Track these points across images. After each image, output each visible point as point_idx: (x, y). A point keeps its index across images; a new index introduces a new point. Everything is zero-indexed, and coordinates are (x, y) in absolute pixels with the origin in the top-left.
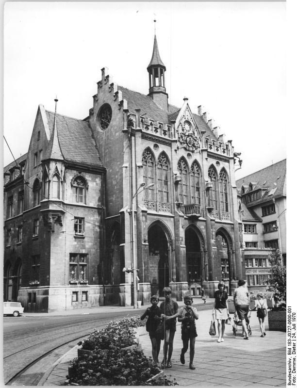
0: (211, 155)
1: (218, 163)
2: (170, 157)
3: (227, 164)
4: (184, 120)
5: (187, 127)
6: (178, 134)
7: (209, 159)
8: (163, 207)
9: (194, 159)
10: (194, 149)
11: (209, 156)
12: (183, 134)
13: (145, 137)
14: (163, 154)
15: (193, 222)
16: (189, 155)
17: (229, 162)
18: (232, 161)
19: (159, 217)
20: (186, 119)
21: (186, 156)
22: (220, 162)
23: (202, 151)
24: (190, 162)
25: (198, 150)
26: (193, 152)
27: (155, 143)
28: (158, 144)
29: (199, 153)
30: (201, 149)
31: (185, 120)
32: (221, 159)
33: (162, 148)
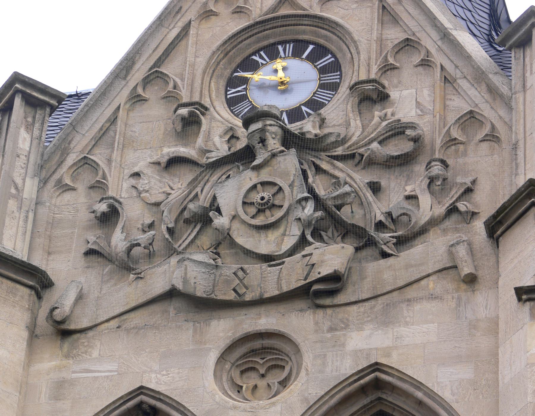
5: (285, 81)
6: (99, 186)
10: (332, 256)
12: (175, 162)
26: (320, 292)
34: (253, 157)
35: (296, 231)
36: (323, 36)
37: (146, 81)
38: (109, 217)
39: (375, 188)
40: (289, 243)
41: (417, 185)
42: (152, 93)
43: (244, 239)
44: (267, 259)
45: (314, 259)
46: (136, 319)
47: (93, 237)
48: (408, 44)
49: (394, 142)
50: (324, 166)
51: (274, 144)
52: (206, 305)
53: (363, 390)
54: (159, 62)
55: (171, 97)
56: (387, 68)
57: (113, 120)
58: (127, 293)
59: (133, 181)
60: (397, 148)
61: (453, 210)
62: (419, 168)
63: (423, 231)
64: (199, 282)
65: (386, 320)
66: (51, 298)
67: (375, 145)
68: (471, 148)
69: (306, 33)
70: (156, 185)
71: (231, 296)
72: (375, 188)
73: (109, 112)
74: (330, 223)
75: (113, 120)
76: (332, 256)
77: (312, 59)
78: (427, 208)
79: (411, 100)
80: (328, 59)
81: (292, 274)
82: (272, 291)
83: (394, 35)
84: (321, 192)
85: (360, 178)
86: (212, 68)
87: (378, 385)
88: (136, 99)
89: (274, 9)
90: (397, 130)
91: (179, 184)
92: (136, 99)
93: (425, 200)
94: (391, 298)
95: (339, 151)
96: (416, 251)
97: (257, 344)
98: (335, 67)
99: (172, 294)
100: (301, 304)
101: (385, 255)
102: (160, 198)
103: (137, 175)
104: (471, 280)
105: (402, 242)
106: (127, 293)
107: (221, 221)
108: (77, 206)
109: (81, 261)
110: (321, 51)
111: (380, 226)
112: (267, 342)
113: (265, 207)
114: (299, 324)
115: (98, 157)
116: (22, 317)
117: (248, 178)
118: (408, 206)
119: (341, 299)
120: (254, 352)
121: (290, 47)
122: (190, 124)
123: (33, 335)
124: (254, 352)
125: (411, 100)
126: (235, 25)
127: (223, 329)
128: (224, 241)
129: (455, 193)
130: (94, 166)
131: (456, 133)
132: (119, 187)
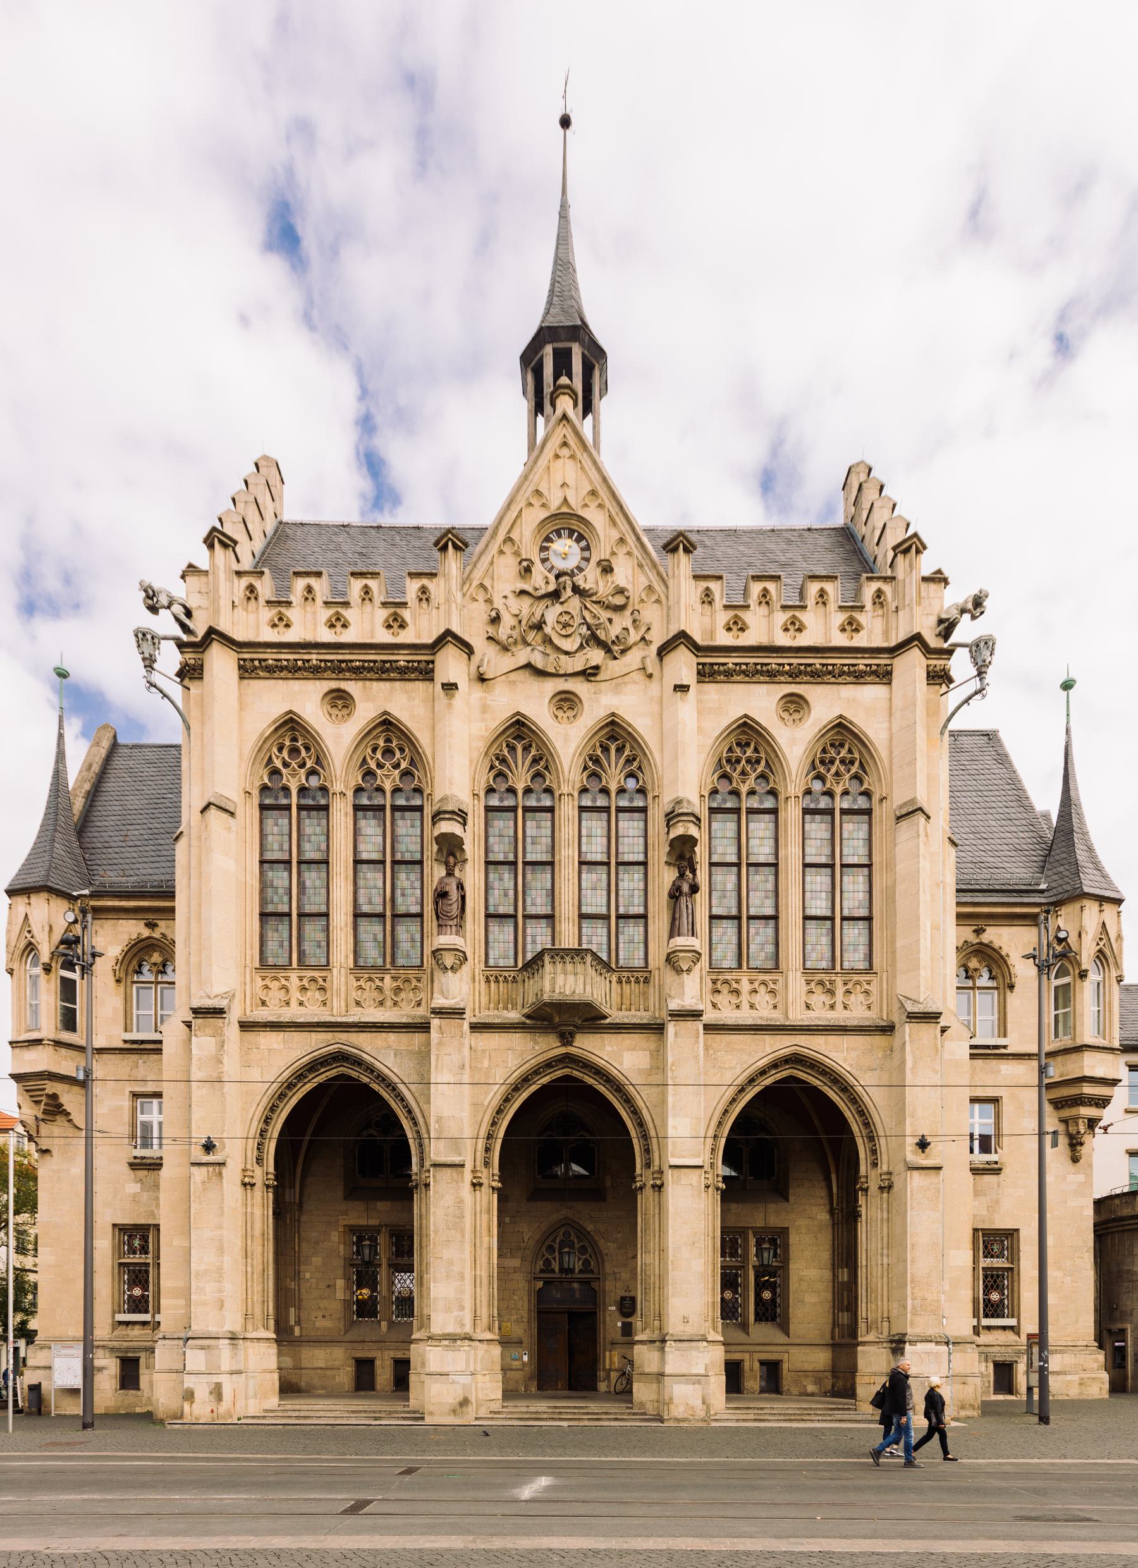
1: (795, 704)
2: (423, 737)
3: (872, 693)
4: (535, 516)
6: (489, 601)
8: (379, 989)
11: (706, 674)
12: (523, 592)
14: (387, 724)
15: (566, 1039)
16: (566, 701)
17: (885, 676)
18: (911, 668)
19: (343, 1037)
20: (555, 503)
22: (813, 693)
24: (568, 741)
25: (633, 659)
26: (590, 673)
27: (334, 685)
28: (352, 687)
29: (639, 677)
31: (544, 514)
33: (372, 699)
34: (559, 597)
35: (579, 640)
36: (582, 528)
37: (505, 542)
39: (610, 620)
40: (576, 646)
43: (557, 641)
44: (567, 653)
45: (588, 656)
47: (491, 631)
49: (617, 596)
50: (588, 606)
52: (541, 673)
53: (607, 725)
54: (509, 532)
55: (517, 553)
56: (613, 553)
57: (492, 563)
58: (508, 662)
59: (504, 600)
60: (619, 600)
61: (643, 639)
62: (628, 612)
63: (630, 648)
64: (539, 661)
65: (617, 690)
67: (610, 598)
68: (649, 604)
70: (513, 602)
71: (553, 671)
72: (610, 620)
73: (489, 558)
74: (593, 639)
75: (492, 563)
78: (634, 637)
81: (577, 664)
82: (570, 671)
85: (604, 615)
87: (613, 723)
89: (559, 508)
90: (621, 591)
91: (524, 606)
92: (501, 552)
93: (631, 630)
95: (594, 598)
97: (563, 696)
99: (529, 666)
100: (581, 679)
101: (615, 658)
102: (517, 612)
103: (505, 597)
104: (650, 676)
105: (623, 652)
106: (508, 662)
108: (480, 612)
109: (485, 642)
111: (613, 642)
112: (567, 696)
114: (578, 686)
118: (625, 632)
119: (598, 678)
120: (561, 700)
121: (567, 532)
124: (561, 700)
125: (624, 573)
127: (552, 686)
128: (548, 640)
129: (643, 629)
130: (485, 589)
131: (644, 596)
132: (498, 603)
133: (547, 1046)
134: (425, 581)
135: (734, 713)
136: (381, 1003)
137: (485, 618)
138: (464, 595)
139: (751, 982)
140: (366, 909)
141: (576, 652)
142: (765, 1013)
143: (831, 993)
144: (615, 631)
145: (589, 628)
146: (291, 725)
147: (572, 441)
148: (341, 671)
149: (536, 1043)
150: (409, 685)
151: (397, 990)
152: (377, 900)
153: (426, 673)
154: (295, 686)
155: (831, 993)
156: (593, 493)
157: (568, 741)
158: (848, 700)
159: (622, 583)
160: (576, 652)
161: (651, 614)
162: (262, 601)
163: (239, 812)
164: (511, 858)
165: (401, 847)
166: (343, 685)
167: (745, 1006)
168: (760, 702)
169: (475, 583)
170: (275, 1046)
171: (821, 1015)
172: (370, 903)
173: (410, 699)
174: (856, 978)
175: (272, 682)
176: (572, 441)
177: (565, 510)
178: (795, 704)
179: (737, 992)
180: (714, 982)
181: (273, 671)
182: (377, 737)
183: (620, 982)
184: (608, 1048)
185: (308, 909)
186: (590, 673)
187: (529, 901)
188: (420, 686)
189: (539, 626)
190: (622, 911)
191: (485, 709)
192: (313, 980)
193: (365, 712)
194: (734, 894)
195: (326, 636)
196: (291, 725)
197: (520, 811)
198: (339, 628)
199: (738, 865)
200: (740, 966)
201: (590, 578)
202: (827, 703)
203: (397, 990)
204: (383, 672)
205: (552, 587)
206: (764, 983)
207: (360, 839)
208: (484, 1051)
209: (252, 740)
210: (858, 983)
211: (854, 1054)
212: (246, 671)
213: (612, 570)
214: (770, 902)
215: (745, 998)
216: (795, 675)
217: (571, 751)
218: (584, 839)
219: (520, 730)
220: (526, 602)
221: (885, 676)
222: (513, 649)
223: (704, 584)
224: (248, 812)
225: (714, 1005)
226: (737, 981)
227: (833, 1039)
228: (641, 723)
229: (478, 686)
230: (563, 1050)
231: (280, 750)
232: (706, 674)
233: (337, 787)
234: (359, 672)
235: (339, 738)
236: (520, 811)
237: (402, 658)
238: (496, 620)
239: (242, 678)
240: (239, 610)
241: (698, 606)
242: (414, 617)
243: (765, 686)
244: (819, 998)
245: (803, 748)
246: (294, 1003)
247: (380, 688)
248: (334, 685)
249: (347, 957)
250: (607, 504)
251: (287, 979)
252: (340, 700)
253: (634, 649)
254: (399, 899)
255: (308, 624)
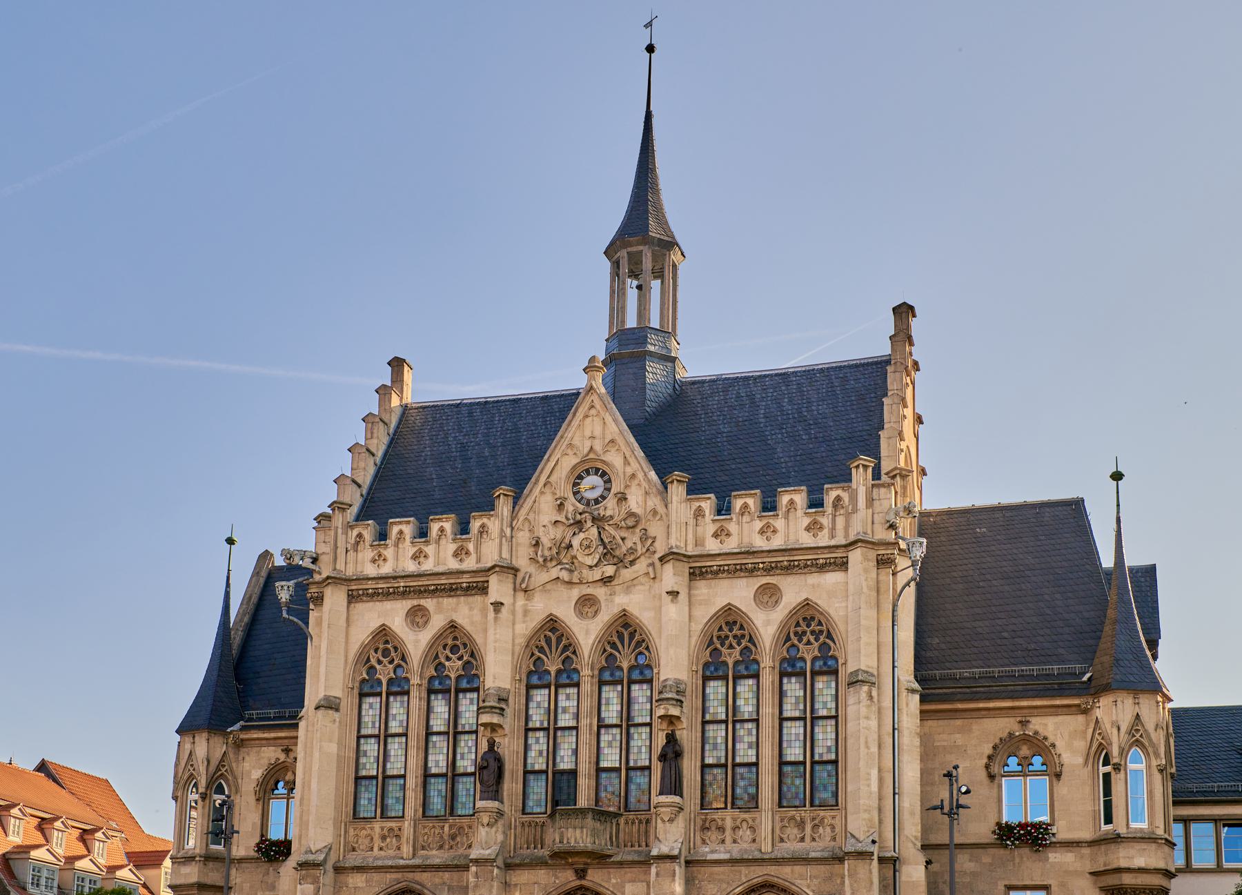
0: (700, 569)
2: (479, 639)
7: (703, 588)
9: (616, 610)
13: (360, 592)
14: (453, 626)
15: (581, 873)
16: (587, 604)
17: (843, 565)
19: (410, 875)
21: (566, 613)
23: (661, 559)
25: (641, 566)
26: (606, 581)
27: (415, 602)
28: (429, 603)
30: (661, 549)
32: (789, 569)
33: (441, 611)
38: (537, 544)
39: (623, 539)
41: (636, 539)
42: (547, 490)
44: (591, 567)
46: (548, 586)
48: (633, 476)
51: (589, 523)
56: (627, 487)
58: (544, 577)
60: (630, 522)
62: (637, 530)
66: (520, 576)
69: (599, 465)
70: (551, 529)
74: (609, 554)
76: (609, 570)
77: (602, 476)
79: (635, 502)
80: (606, 478)
81: (597, 574)
83: (629, 471)
84: (606, 541)
85: (617, 535)
86: (568, 478)
88: (542, 493)
90: (631, 514)
92: (542, 493)
93: (639, 547)
94: (630, 586)
96: (636, 567)
98: (609, 481)
105: (632, 563)
107: (574, 552)
110: (604, 474)
113: (588, 547)
114: (600, 592)
115: (531, 517)
116: (511, 586)
117: (582, 535)
122: (561, 507)
123: (515, 590)
125: (635, 502)
126: (575, 461)
127: (576, 593)
129: (650, 541)
132: (540, 532)
133: (567, 878)
134: (485, 520)
135: (720, 602)
136: (441, 847)
137: (527, 542)
138: (512, 529)
139: (734, 820)
140: (434, 771)
141: (596, 565)
142: (742, 848)
143: (801, 825)
144: (629, 544)
145: (605, 547)
146: (383, 633)
147: (598, 404)
148: (420, 592)
149: (557, 878)
150: (470, 599)
151: (453, 837)
152: (443, 764)
153: (483, 589)
154: (388, 605)
155: (801, 825)
156: (612, 441)
157: (587, 635)
158: (813, 586)
159: (635, 509)
160: (596, 565)
161: (655, 529)
162: (367, 544)
163: (343, 705)
164: (546, 725)
165: (462, 721)
166: (422, 602)
167: (728, 840)
168: (739, 593)
169: (521, 519)
170: (360, 885)
171: (792, 846)
172: (437, 766)
173: (471, 609)
174: (822, 813)
175: (371, 604)
176: (598, 404)
177: (592, 456)
178: (769, 595)
179: (721, 829)
180: (704, 821)
181: (375, 595)
182: (446, 637)
183: (627, 823)
184: (614, 881)
185: (389, 773)
186: (606, 581)
187: (558, 760)
188: (478, 598)
189: (570, 546)
190: (632, 764)
191: (526, 612)
192: (391, 829)
193: (438, 622)
194: (723, 747)
195: (411, 567)
196: (383, 633)
197: (553, 688)
198: (422, 559)
199: (726, 722)
200: (726, 808)
201: (610, 507)
202: (794, 590)
203: (453, 837)
204: (451, 590)
205: (578, 517)
206: (744, 820)
207: (432, 716)
208: (516, 885)
209: (354, 648)
210: (823, 818)
211: (816, 882)
212: (352, 598)
213: (626, 499)
214: (752, 752)
215: (728, 832)
216: (770, 570)
217: (591, 642)
218: (603, 708)
219: (552, 625)
220: (561, 529)
221: (843, 565)
222: (549, 565)
223: (697, 504)
224: (349, 704)
225: (704, 842)
226: (723, 820)
227: (798, 869)
228: (643, 615)
229: (520, 595)
230: (578, 883)
231: (376, 651)
232: (696, 574)
233: (415, 680)
234: (437, 591)
235: (416, 643)
236: (553, 688)
237: (465, 579)
238: (537, 544)
239: (349, 602)
240: (351, 553)
241: (692, 522)
242: (477, 548)
243: (745, 580)
244: (793, 832)
245: (776, 627)
246: (376, 849)
247: (448, 602)
248: (415, 602)
249: (416, 811)
250: (623, 448)
251: (372, 829)
252: (417, 617)
253: (642, 558)
254: (459, 763)
255: (400, 557)
